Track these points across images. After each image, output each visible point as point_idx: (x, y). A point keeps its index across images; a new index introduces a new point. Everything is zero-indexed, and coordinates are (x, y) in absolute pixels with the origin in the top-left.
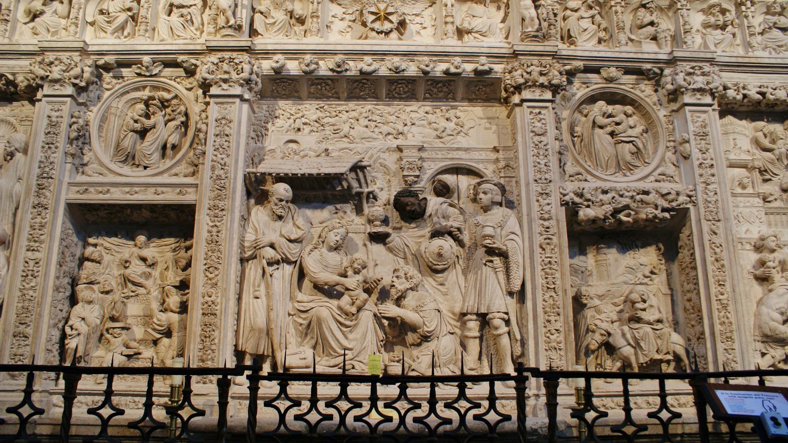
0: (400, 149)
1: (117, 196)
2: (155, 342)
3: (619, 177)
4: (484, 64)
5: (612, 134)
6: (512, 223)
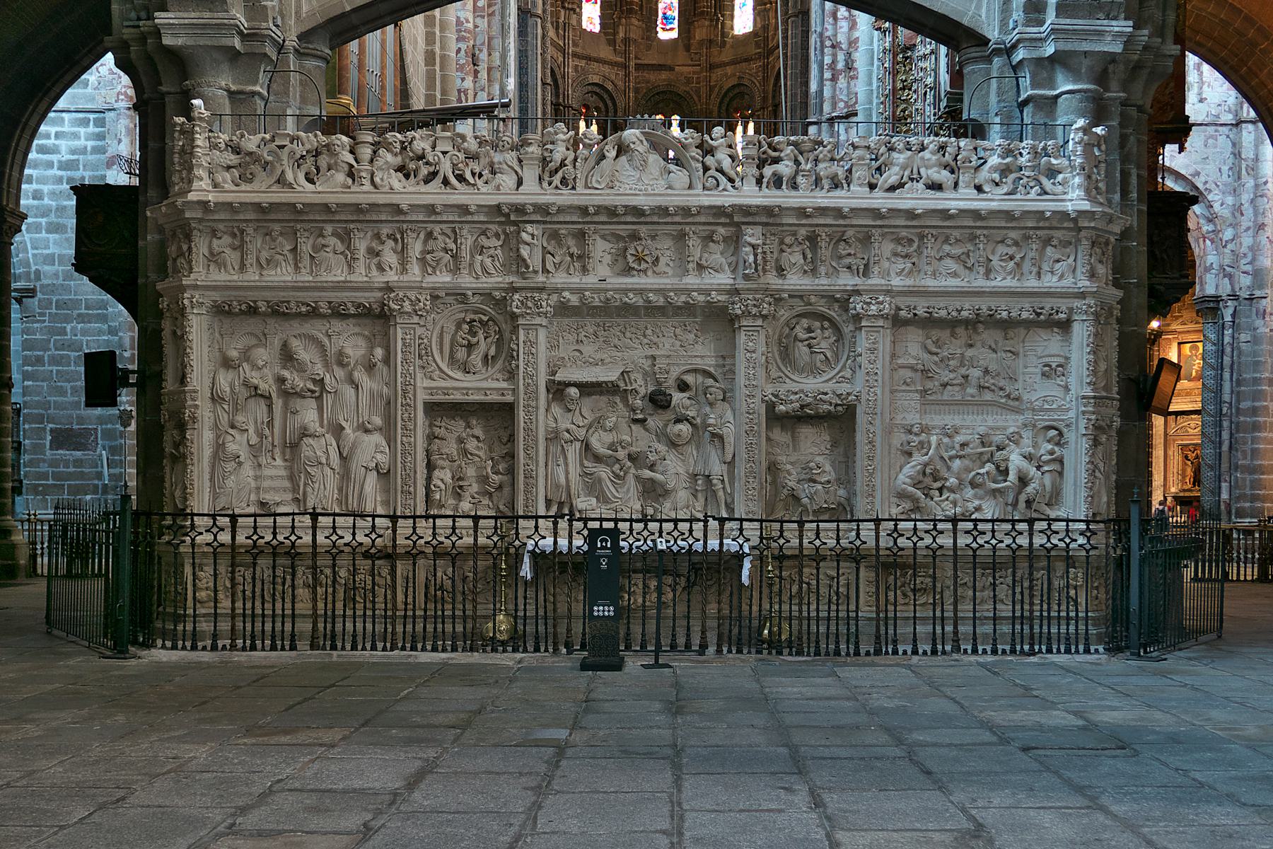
0: (654, 358)
1: (457, 397)
3: (811, 380)
5: (810, 346)
6: (729, 415)
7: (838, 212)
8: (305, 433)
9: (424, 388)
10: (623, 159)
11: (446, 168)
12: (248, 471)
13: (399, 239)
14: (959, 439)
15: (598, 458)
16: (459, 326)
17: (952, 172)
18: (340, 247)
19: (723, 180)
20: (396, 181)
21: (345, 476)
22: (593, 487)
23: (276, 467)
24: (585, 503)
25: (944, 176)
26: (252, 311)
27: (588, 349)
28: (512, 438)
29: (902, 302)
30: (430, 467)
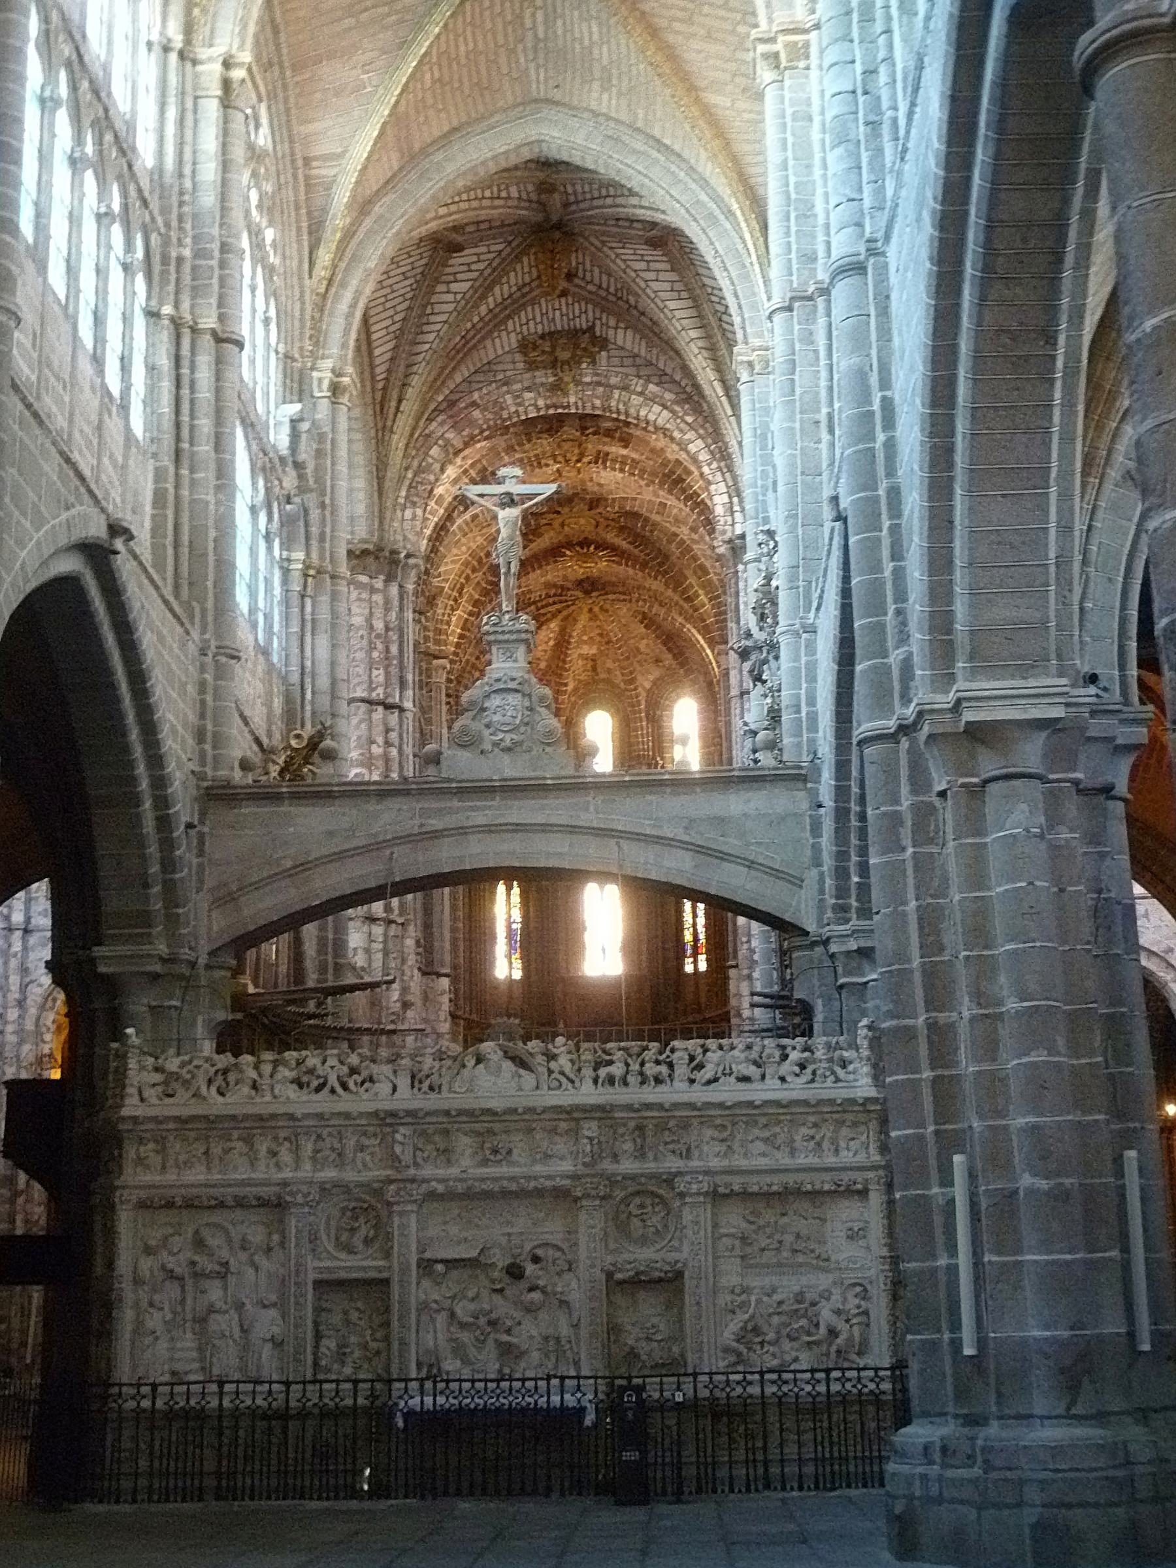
0: (509, 1234)
1: (343, 1275)
2: (370, 1360)
4: (559, 1182)
5: (643, 1221)
6: (574, 1285)
7: (660, 1106)
8: (211, 1310)
9: (314, 1268)
10: (481, 1066)
11: (333, 1080)
12: (163, 1345)
13: (294, 1140)
14: (777, 1297)
15: (463, 1326)
16: (344, 1210)
17: (759, 1066)
18: (245, 1150)
19: (564, 1080)
20: (292, 1092)
21: (246, 1347)
22: (458, 1350)
23: (188, 1341)
24: (451, 1365)
25: (752, 1071)
26: (170, 1205)
27: (454, 1230)
28: (387, 1310)
29: (718, 1179)
30: (318, 1336)
